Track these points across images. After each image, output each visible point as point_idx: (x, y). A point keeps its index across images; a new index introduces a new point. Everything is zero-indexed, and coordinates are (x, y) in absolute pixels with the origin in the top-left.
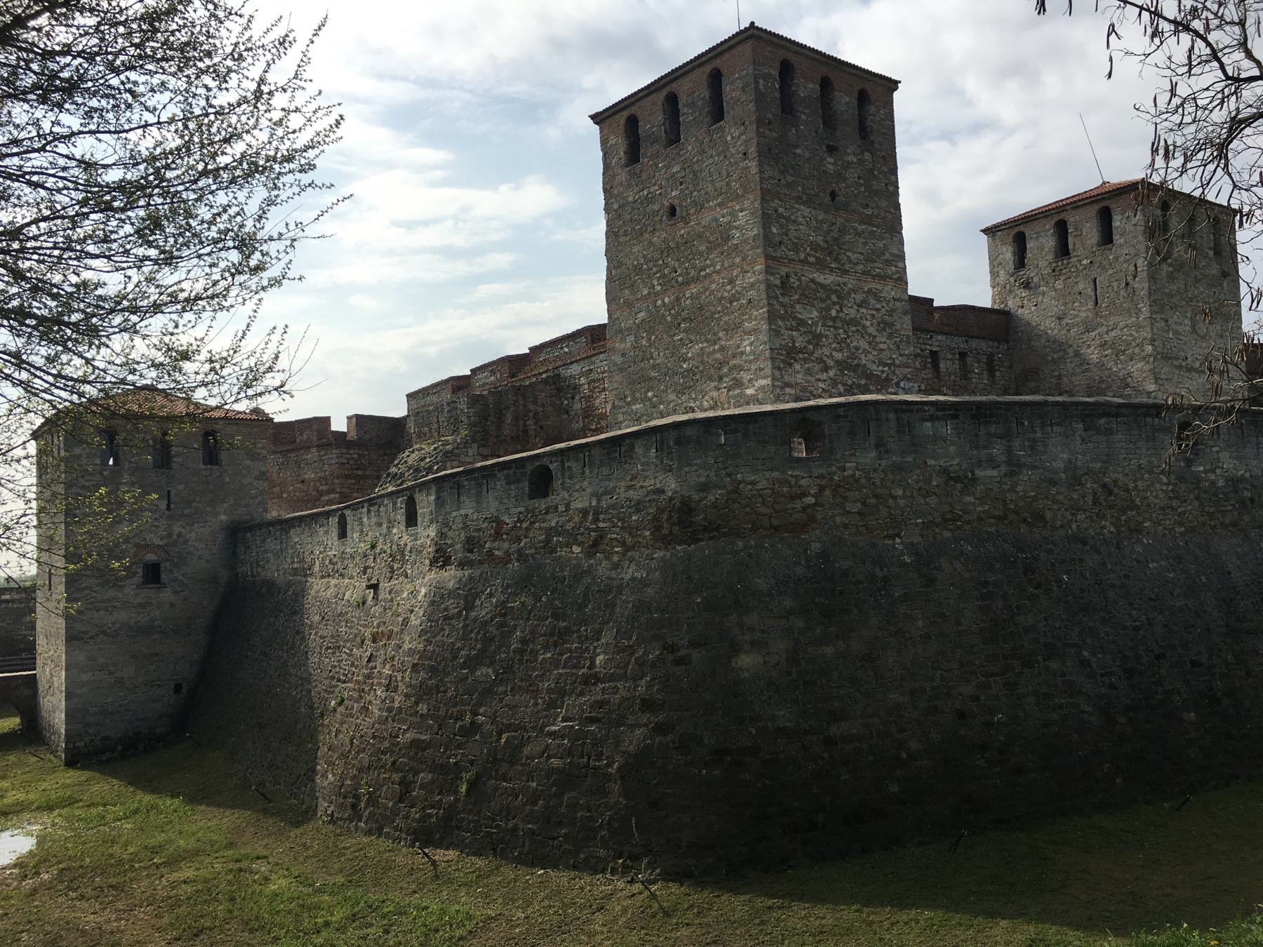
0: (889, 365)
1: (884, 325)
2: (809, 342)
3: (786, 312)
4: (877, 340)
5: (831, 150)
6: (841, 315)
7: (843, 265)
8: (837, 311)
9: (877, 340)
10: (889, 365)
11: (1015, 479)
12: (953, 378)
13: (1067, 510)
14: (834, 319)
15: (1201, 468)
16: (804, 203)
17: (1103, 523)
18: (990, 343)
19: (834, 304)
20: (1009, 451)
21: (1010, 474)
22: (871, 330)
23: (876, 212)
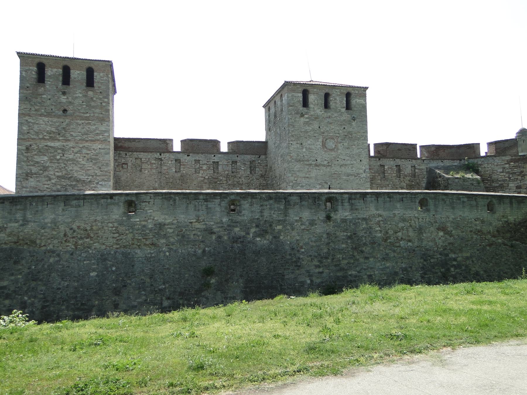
0: (92, 176)
1: (90, 160)
2: (41, 170)
3: (28, 159)
4: (86, 166)
5: (64, 93)
6: (63, 158)
7: (67, 138)
8: (61, 157)
9: (86, 166)
10: (92, 176)
11: (25, 227)
12: (227, 172)
13: (48, 239)
14: (58, 160)
15: (138, 220)
16: (45, 116)
17: (68, 244)
18: (254, 156)
19: (59, 153)
20: (24, 216)
21: (22, 225)
22: (83, 162)
23: (92, 115)
